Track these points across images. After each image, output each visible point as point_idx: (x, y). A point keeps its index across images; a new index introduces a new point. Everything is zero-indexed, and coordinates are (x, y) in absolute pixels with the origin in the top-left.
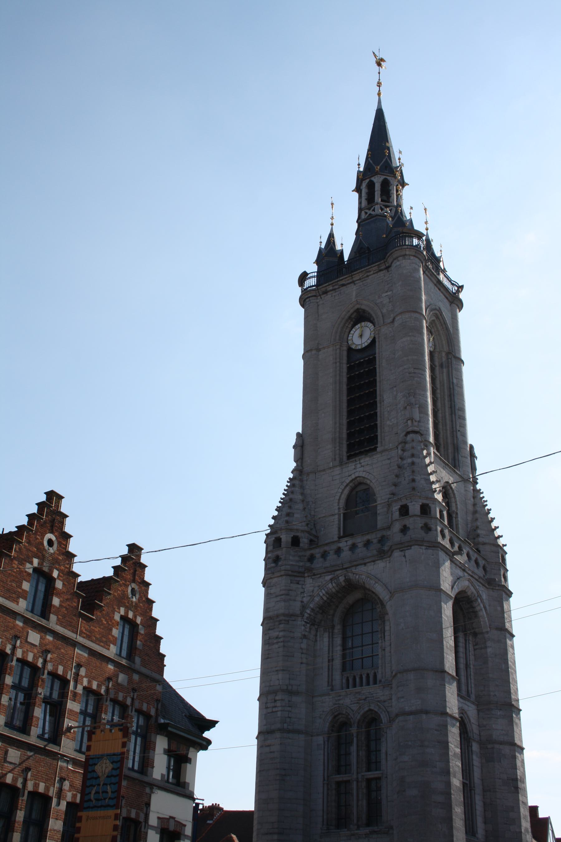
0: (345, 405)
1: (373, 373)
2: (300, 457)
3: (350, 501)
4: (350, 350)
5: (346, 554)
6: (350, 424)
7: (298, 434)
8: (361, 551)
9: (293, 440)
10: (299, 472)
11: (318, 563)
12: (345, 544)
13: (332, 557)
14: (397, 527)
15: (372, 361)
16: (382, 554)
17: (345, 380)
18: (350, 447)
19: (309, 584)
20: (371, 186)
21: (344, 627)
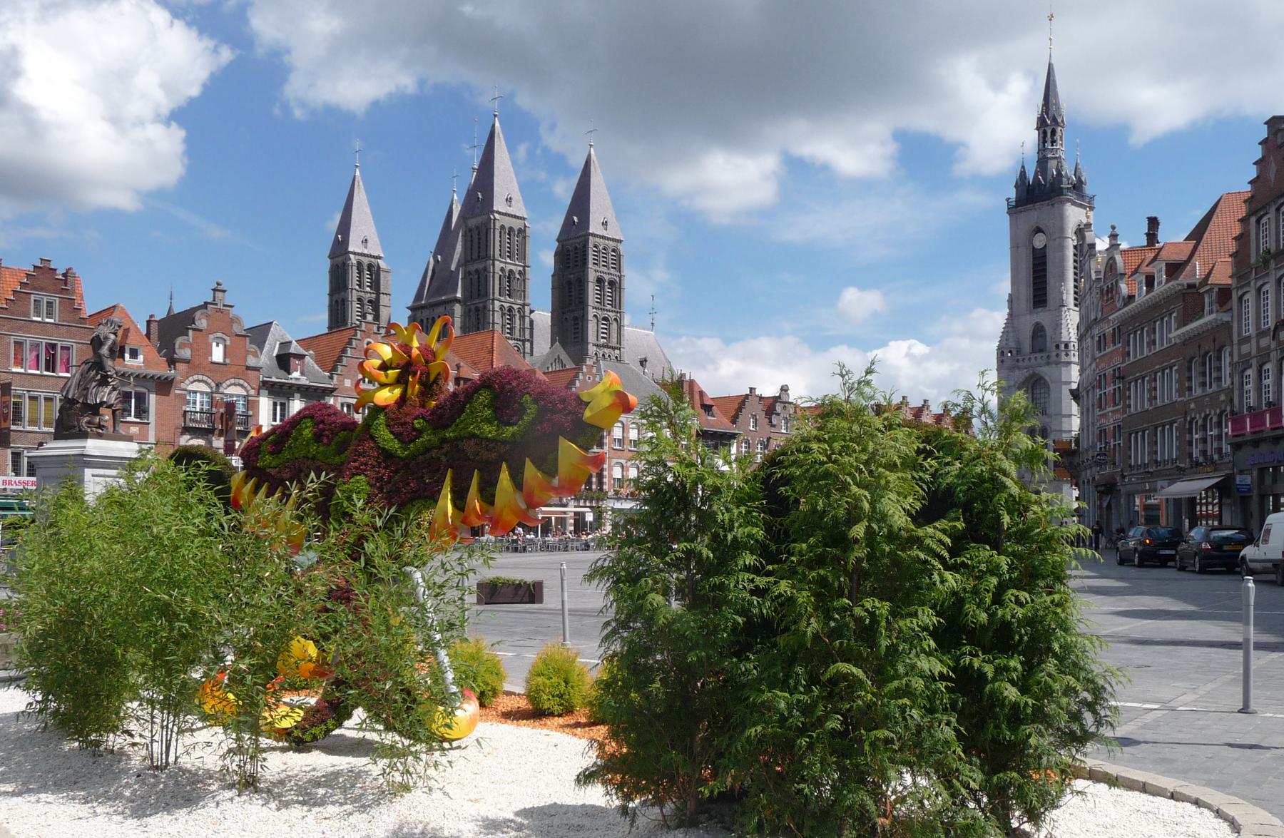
0: (1032, 279)
1: (1045, 263)
2: (1011, 308)
3: (1034, 332)
4: (1034, 247)
5: (1033, 360)
6: (1034, 290)
7: (1010, 295)
8: (1039, 360)
9: (1007, 297)
10: (1010, 314)
11: (1021, 364)
12: (1032, 356)
13: (1026, 361)
14: (1054, 354)
15: (1045, 256)
16: (1048, 364)
17: (1031, 266)
18: (1034, 302)
19: (1017, 372)
20: (1045, 133)
21: (1033, 390)
